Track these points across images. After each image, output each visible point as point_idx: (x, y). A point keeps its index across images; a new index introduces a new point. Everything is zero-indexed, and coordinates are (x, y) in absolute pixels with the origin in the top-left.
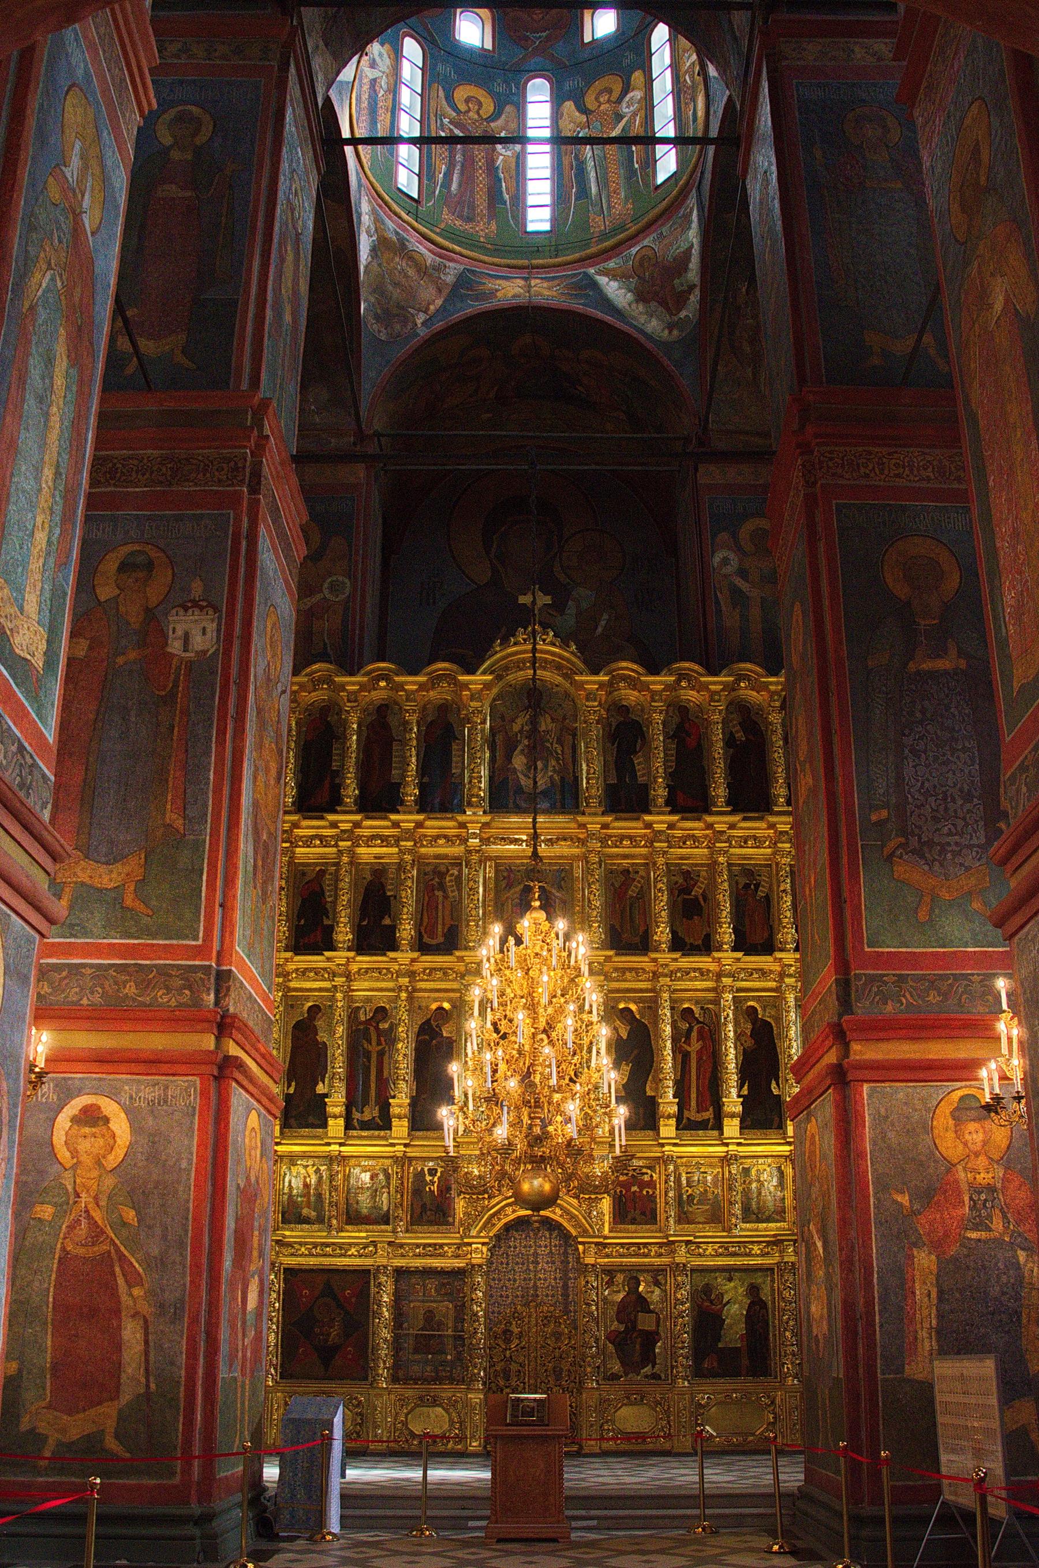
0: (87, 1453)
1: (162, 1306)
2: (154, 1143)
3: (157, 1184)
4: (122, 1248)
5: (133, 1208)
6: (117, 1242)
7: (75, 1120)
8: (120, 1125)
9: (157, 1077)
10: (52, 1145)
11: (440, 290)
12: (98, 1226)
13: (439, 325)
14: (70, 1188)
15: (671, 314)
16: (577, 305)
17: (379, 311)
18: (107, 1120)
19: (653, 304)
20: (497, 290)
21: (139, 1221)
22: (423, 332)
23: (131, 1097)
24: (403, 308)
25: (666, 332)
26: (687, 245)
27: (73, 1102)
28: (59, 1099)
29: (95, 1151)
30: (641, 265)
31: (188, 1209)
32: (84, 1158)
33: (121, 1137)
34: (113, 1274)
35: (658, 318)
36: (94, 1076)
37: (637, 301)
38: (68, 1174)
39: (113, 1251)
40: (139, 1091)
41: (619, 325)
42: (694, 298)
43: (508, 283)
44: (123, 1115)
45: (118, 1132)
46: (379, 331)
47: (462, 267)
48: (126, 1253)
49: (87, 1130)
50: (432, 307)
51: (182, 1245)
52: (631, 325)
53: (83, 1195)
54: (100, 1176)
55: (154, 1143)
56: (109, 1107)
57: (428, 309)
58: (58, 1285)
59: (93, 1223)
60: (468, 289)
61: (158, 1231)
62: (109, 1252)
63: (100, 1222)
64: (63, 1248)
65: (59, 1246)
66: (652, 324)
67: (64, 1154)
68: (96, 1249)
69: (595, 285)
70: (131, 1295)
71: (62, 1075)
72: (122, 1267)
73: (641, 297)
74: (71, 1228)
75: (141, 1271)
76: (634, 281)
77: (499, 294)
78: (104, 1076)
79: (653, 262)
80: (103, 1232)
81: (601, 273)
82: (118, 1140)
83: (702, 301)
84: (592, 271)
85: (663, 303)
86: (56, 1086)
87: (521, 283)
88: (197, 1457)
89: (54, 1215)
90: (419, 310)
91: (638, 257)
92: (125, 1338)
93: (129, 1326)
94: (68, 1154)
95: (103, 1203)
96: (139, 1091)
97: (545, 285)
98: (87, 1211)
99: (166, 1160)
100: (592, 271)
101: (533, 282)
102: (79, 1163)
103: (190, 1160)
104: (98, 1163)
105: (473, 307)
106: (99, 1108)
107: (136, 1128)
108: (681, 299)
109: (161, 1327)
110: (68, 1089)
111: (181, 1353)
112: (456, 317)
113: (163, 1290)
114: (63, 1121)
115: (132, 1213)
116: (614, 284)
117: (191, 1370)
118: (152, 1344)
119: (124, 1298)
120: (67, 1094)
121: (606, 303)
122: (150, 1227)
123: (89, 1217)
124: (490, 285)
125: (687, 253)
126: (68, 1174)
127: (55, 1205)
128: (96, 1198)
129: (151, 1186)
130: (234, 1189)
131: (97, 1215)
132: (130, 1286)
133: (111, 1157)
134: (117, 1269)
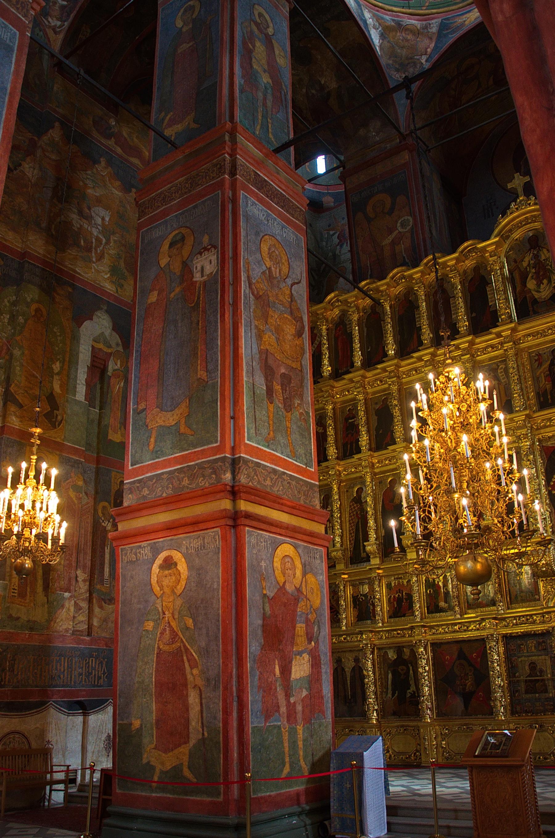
0: (173, 779)
1: (208, 680)
2: (199, 574)
3: (202, 600)
4: (187, 644)
5: (191, 617)
6: (184, 640)
7: (161, 567)
8: (182, 567)
9: (198, 533)
10: (151, 584)
11: (431, 39)
12: (174, 632)
13: (436, 57)
14: (160, 609)
18: (176, 564)
20: (464, 21)
21: (194, 626)
23: (187, 548)
24: (411, 58)
27: (159, 556)
28: (153, 556)
29: (171, 584)
31: (219, 614)
32: (167, 590)
33: (183, 573)
34: (183, 661)
36: (168, 538)
38: (159, 601)
39: (182, 646)
40: (190, 543)
43: (471, 14)
44: (183, 560)
45: (182, 571)
47: (440, 19)
48: (189, 647)
49: (167, 572)
50: (429, 50)
51: (217, 637)
53: (167, 613)
54: (174, 600)
55: (199, 574)
56: (177, 556)
57: (426, 52)
58: (157, 670)
59: (172, 631)
60: (447, 29)
61: (204, 631)
62: (180, 647)
63: (175, 629)
64: (159, 647)
65: (156, 646)
67: (157, 589)
68: (174, 646)
70: (192, 674)
71: (155, 541)
72: (187, 656)
74: (162, 634)
75: (197, 658)
77: (466, 23)
78: (173, 537)
80: (177, 635)
82: (182, 575)
86: (151, 548)
88: (236, 782)
89: (154, 627)
92: (190, 702)
93: (192, 695)
94: (158, 588)
95: (176, 617)
96: (190, 543)
98: (169, 623)
99: (206, 584)
102: (164, 592)
103: (218, 582)
104: (173, 591)
105: (453, 37)
106: (172, 557)
107: (190, 567)
109: (208, 694)
110: (157, 549)
111: (220, 711)
112: (445, 48)
113: (208, 669)
114: (155, 568)
115: (191, 621)
117: (226, 723)
118: (204, 705)
119: (189, 676)
120: (156, 552)
122: (200, 629)
123: (170, 626)
124: (460, 20)
126: (159, 601)
127: (154, 620)
128: (173, 614)
129: (199, 602)
130: (258, 597)
131: (173, 624)
132: (192, 669)
133: (179, 587)
134: (185, 658)
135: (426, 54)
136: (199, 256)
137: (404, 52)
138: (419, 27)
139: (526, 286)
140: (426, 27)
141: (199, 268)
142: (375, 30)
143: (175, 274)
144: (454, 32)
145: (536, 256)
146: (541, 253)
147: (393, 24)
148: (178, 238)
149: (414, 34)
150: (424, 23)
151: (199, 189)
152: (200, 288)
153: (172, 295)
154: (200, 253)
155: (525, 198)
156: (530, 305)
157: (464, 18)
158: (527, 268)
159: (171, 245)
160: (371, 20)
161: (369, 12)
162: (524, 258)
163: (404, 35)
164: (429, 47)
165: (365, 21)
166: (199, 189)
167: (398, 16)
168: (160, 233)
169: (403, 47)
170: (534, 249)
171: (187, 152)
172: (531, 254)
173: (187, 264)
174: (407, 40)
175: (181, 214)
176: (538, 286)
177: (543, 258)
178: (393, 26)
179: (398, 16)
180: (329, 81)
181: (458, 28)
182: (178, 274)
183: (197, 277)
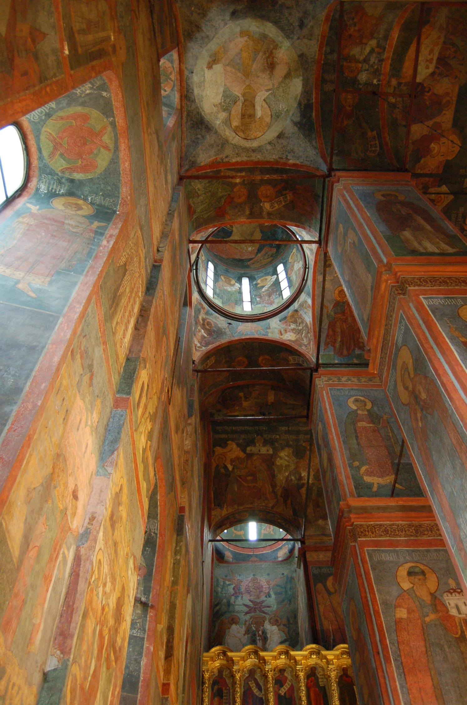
136: (449, 595)
141: (453, 604)
143: (423, 600)
148: (417, 570)
151: (425, 538)
152: (460, 623)
153: (427, 619)
154: (451, 593)
159: (410, 574)
166: (425, 538)
168: (391, 559)
171: (401, 503)
173: (436, 597)
175: (413, 551)
182: (429, 602)
183: (453, 612)
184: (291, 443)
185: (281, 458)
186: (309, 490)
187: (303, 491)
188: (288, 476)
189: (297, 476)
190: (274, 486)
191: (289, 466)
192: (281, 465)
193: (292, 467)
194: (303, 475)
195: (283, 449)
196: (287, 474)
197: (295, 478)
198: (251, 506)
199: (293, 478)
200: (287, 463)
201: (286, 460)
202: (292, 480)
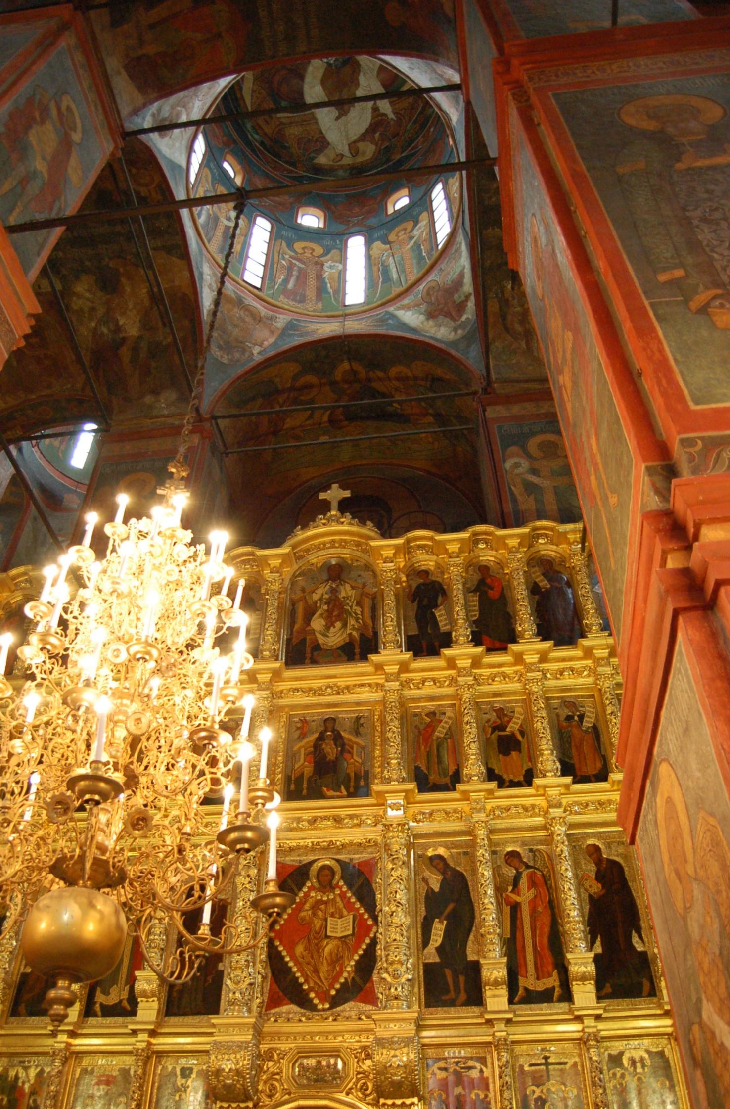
11: (272, 332)
13: (272, 353)
15: (454, 320)
16: (382, 331)
17: (221, 343)
19: (441, 318)
22: (258, 358)
24: (241, 343)
25: (453, 334)
26: (461, 268)
30: (428, 294)
35: (445, 326)
37: (428, 319)
41: (414, 337)
42: (471, 304)
43: (326, 325)
46: (222, 357)
50: (266, 343)
52: (425, 336)
66: (441, 332)
69: (393, 316)
73: (431, 315)
76: (423, 307)
79: (437, 288)
81: (399, 309)
83: (477, 304)
84: (391, 309)
85: (448, 315)
87: (338, 324)
90: (255, 344)
91: (425, 290)
97: (356, 323)
100: (391, 309)
101: (346, 323)
108: (461, 307)
116: (409, 313)
121: (403, 326)
124: (313, 327)
125: (462, 275)
135: (260, 346)
137: (236, 332)
138: (262, 314)
139: (309, 624)
140: (271, 318)
142: (209, 291)
144: (301, 335)
145: (334, 591)
146: (342, 588)
147: (233, 295)
149: (255, 319)
150: (271, 313)
155: (339, 514)
156: (308, 650)
157: (318, 326)
158: (316, 603)
160: (208, 277)
161: (211, 268)
162: (317, 588)
163: (242, 314)
164: (267, 340)
165: (201, 278)
167: (243, 292)
169: (236, 326)
170: (334, 580)
172: (328, 587)
174: (244, 321)
176: (328, 628)
177: (343, 594)
178: (232, 298)
179: (243, 292)
180: (130, 325)
181: (307, 334)
184: (87, 263)
185: (79, 296)
186: (135, 349)
187: (125, 353)
188: (95, 329)
189: (112, 327)
190: (75, 349)
191: (93, 309)
192: (82, 310)
193: (101, 311)
194: (121, 323)
195: (77, 278)
196: (93, 324)
197: (109, 330)
198: (49, 392)
199: (105, 331)
200: (89, 304)
201: (87, 299)
202: (102, 333)
